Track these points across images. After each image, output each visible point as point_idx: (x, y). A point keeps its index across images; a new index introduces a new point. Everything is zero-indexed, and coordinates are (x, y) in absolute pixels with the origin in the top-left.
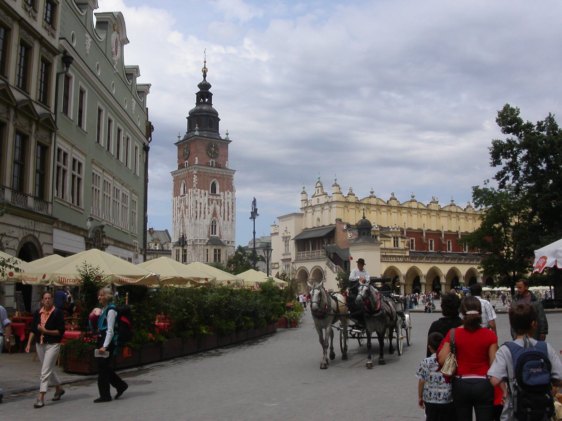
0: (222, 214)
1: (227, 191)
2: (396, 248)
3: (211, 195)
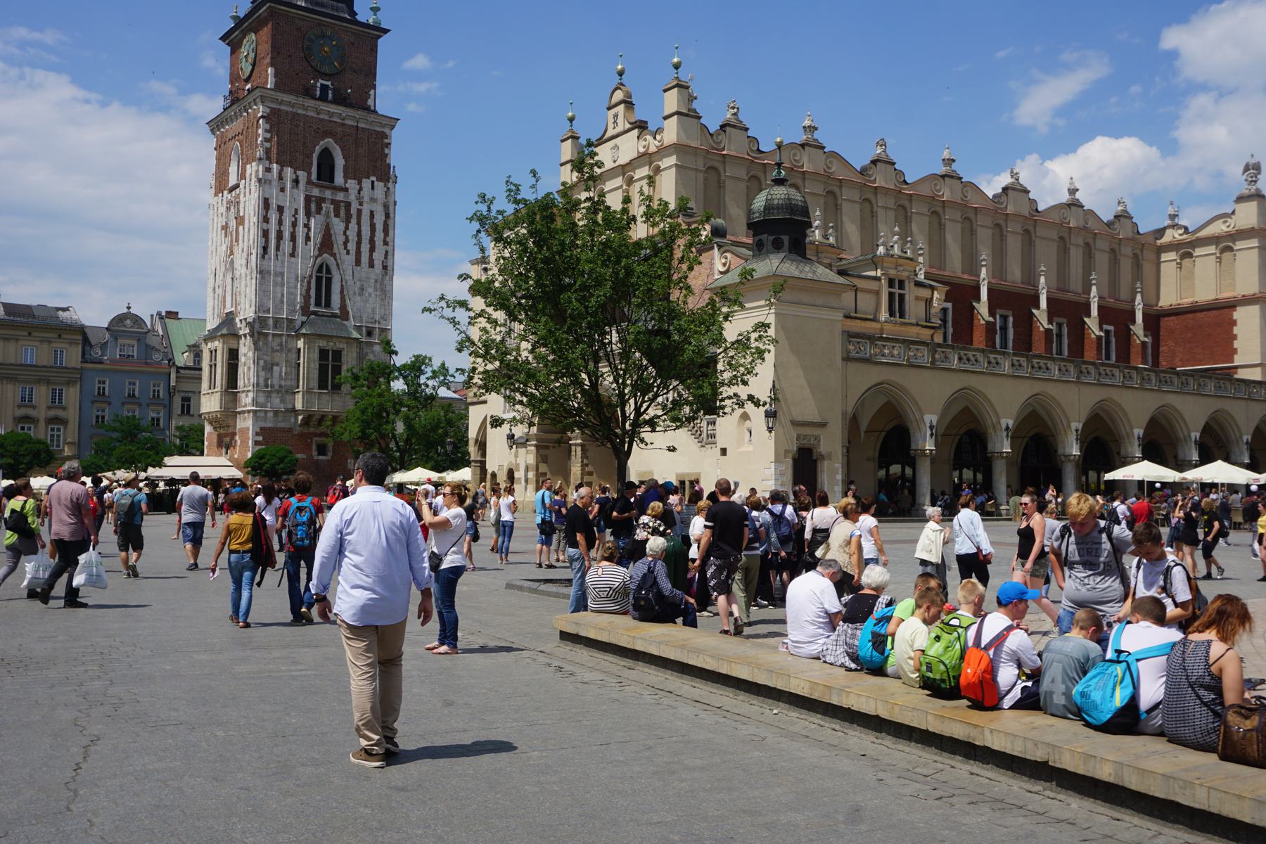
0: (352, 246)
1: (368, 178)
2: (897, 319)
3: (317, 186)
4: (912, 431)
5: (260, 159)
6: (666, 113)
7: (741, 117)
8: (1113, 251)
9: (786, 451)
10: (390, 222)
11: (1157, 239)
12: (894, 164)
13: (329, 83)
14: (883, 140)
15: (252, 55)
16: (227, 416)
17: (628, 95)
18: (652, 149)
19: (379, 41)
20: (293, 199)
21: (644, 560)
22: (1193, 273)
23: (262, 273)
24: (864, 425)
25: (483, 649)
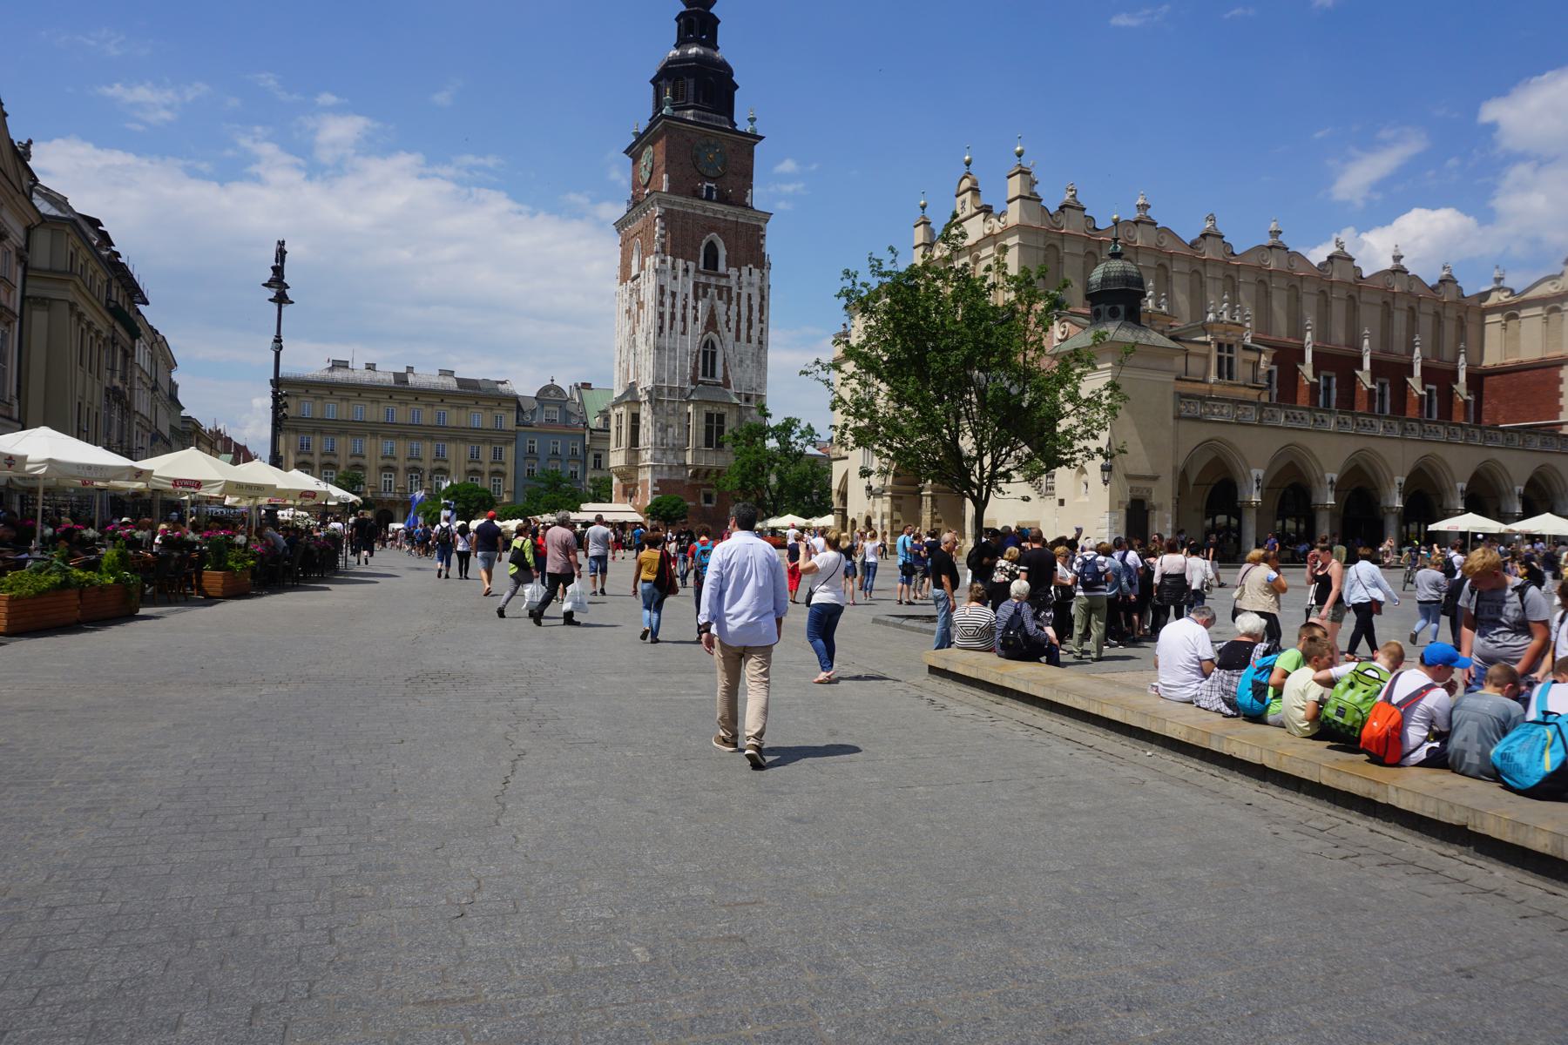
0: (733, 324)
1: (746, 265)
2: (1226, 381)
3: (704, 273)
4: (1238, 485)
5: (657, 252)
6: (1010, 197)
7: (1079, 198)
8: (1437, 314)
9: (1120, 502)
10: (765, 303)
11: (1481, 302)
12: (1223, 237)
13: (713, 185)
14: (1212, 215)
15: (650, 165)
16: (630, 470)
17: (975, 183)
18: (997, 230)
19: (756, 147)
20: (684, 285)
21: (1009, 601)
22: (1518, 334)
23: (659, 349)
24: (1192, 479)
25: (858, 678)
